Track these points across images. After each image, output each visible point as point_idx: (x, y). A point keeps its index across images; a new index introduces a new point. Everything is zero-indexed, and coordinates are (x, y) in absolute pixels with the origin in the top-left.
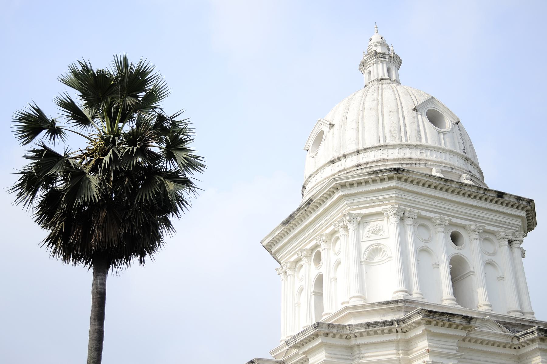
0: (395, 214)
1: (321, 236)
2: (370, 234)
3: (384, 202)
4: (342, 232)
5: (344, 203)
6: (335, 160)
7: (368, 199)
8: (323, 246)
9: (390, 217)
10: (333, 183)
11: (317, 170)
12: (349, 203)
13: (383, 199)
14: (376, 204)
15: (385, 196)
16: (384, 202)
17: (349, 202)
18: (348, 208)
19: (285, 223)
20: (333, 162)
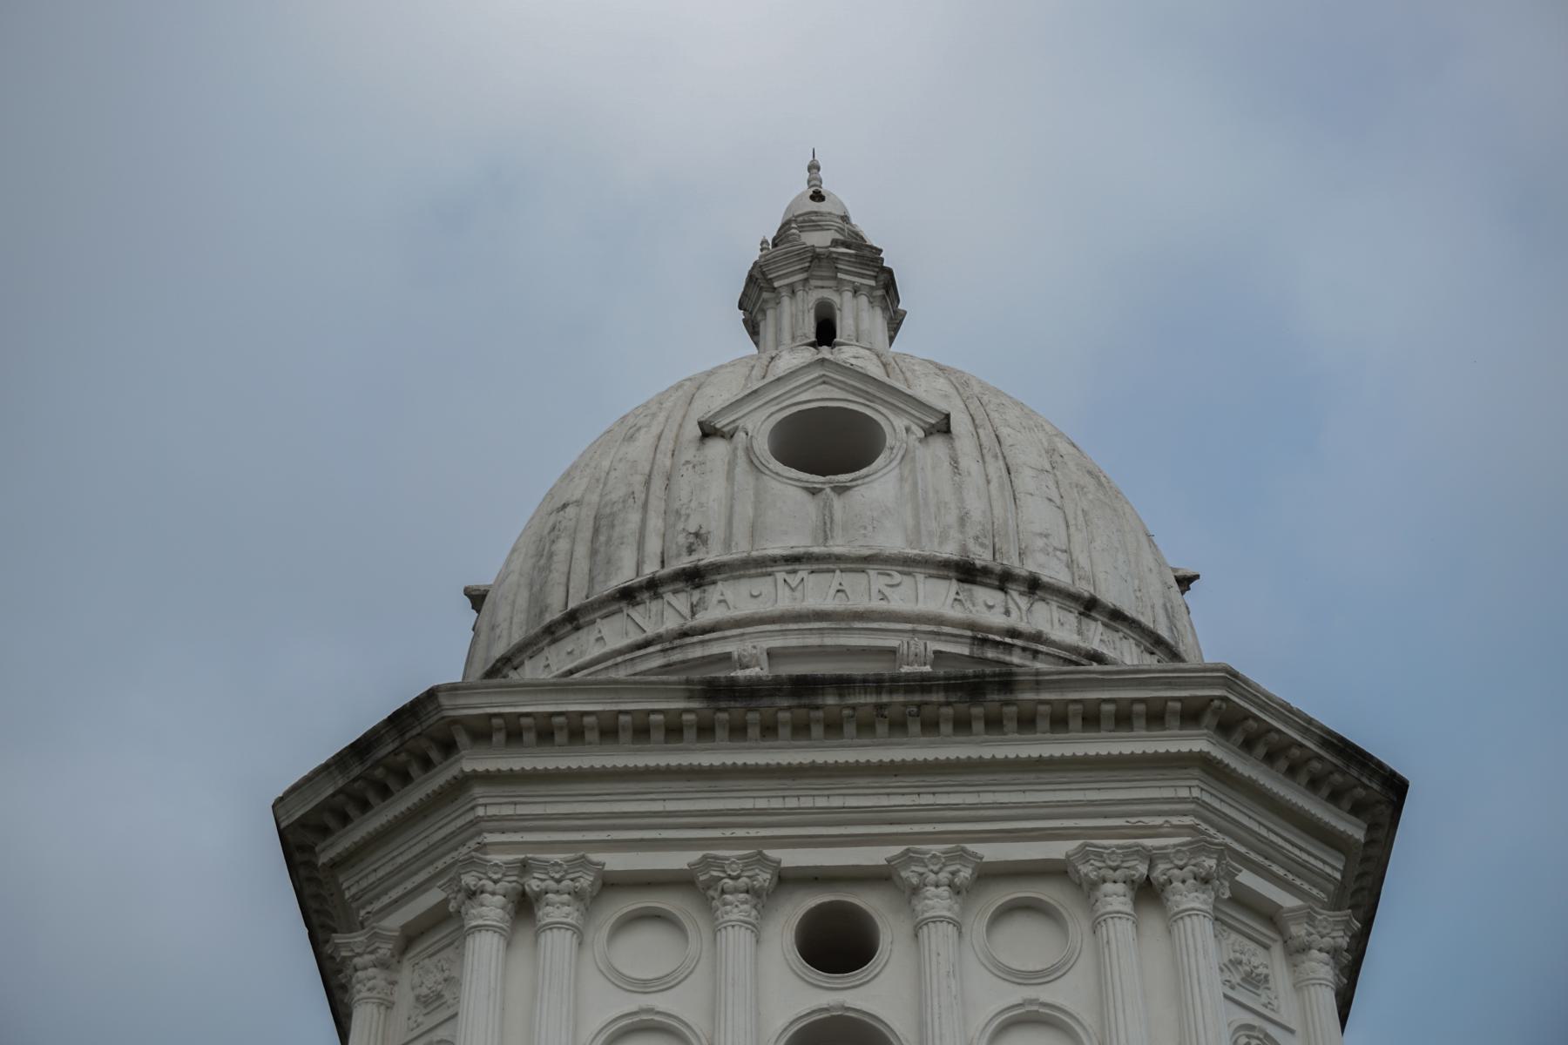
0: (1334, 952)
1: (951, 857)
2: (1236, 979)
3: (1298, 882)
4: (1116, 898)
5: (1188, 788)
6: (986, 571)
7: (1264, 832)
8: (937, 902)
9: (1315, 953)
10: (1211, 685)
11: (867, 560)
12: (1205, 805)
13: (1304, 865)
14: (1275, 868)
15: (1312, 860)
16: (1298, 882)
17: (1206, 798)
18: (1188, 820)
19: (717, 691)
20: (967, 573)
